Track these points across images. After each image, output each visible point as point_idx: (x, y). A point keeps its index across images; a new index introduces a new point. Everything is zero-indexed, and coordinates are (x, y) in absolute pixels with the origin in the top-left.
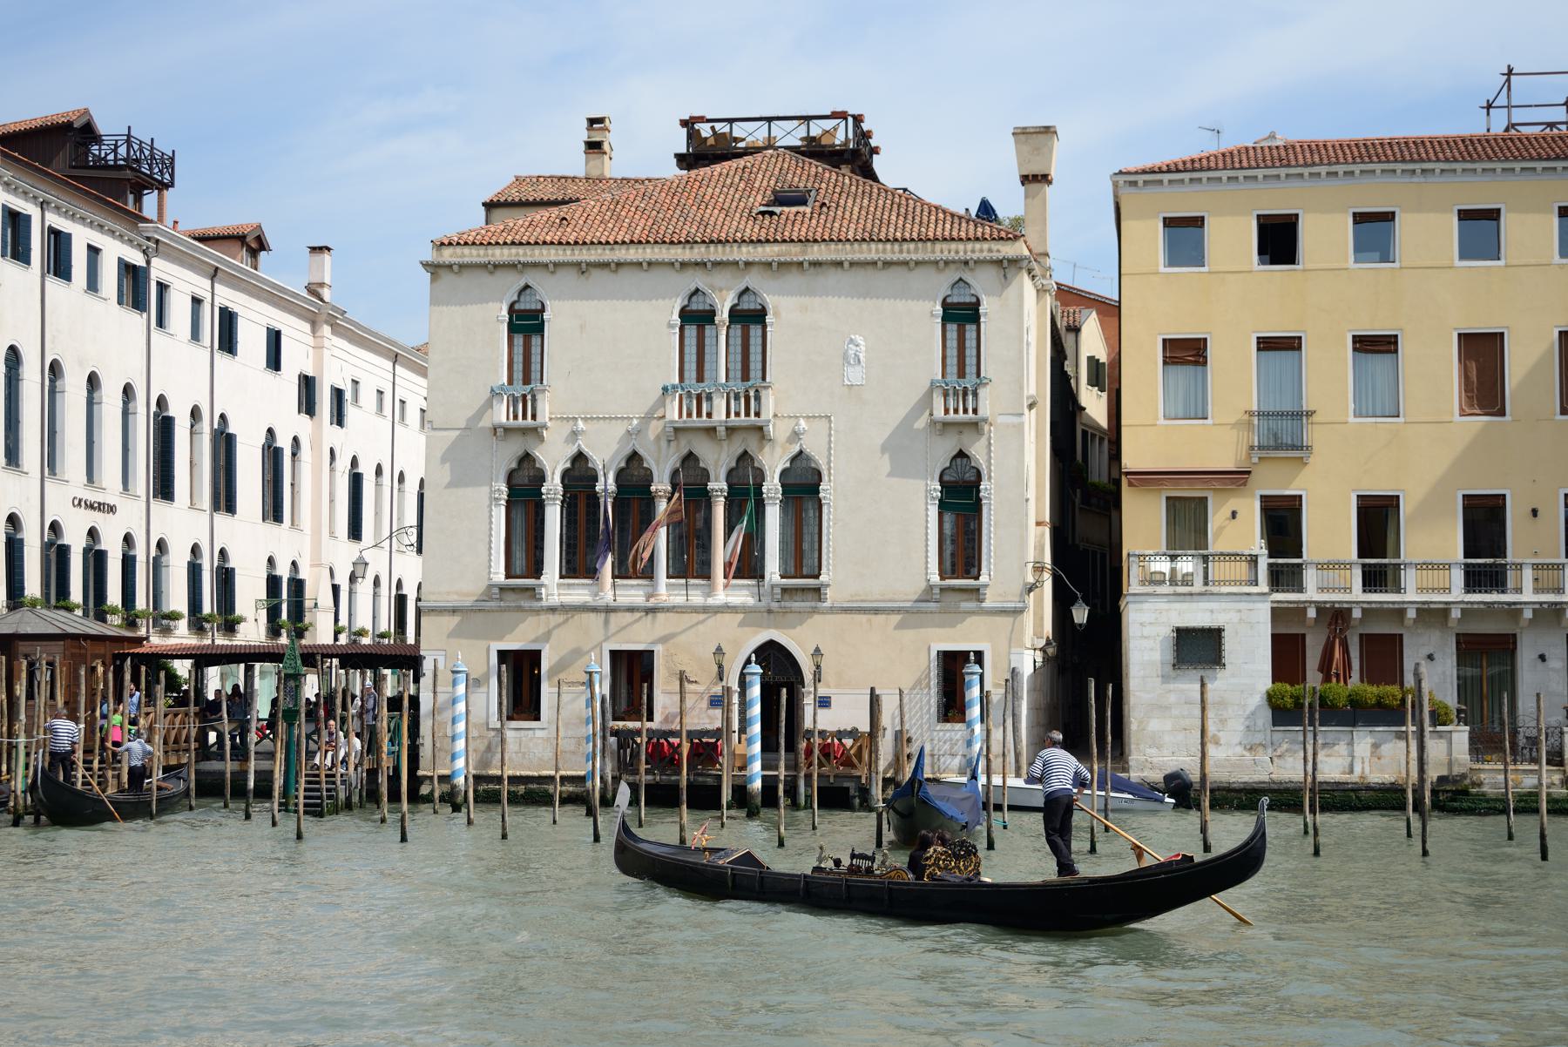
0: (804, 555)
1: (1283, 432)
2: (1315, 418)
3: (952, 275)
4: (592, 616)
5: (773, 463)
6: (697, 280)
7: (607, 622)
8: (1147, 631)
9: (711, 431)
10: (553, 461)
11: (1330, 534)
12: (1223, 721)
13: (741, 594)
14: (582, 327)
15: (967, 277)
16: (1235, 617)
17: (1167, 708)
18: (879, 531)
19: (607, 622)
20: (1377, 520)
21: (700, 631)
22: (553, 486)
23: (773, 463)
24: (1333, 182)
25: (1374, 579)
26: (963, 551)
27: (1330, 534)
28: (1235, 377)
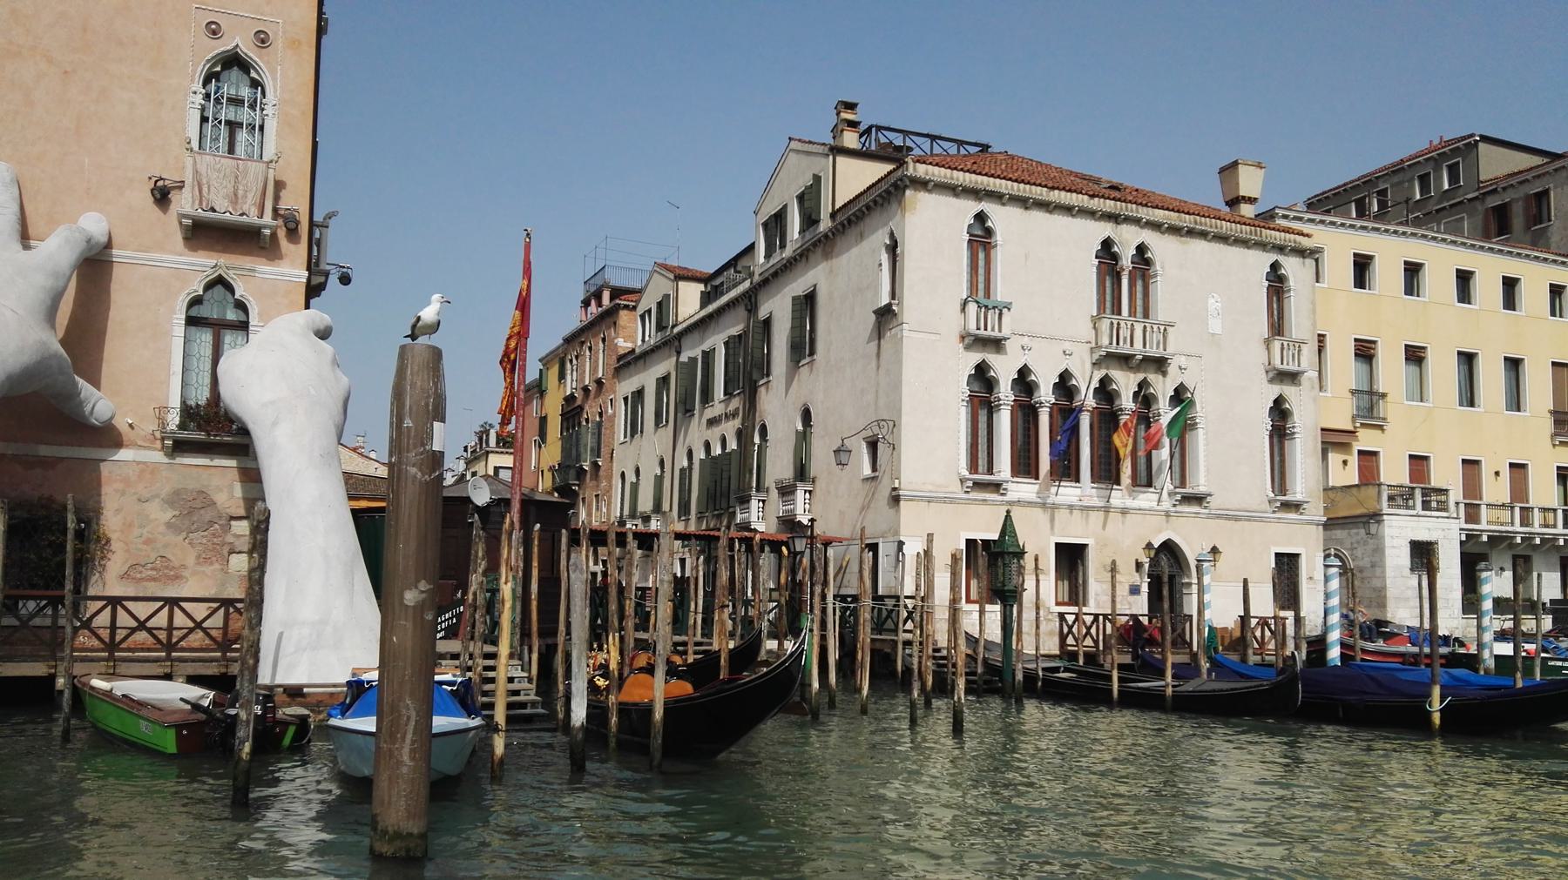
2: (1389, 398)
5: (1162, 388)
6: (1105, 230)
7: (1052, 520)
13: (1146, 499)
14: (1026, 257)
17: (1407, 599)
19: (1052, 520)
21: (1118, 527)
22: (1005, 392)
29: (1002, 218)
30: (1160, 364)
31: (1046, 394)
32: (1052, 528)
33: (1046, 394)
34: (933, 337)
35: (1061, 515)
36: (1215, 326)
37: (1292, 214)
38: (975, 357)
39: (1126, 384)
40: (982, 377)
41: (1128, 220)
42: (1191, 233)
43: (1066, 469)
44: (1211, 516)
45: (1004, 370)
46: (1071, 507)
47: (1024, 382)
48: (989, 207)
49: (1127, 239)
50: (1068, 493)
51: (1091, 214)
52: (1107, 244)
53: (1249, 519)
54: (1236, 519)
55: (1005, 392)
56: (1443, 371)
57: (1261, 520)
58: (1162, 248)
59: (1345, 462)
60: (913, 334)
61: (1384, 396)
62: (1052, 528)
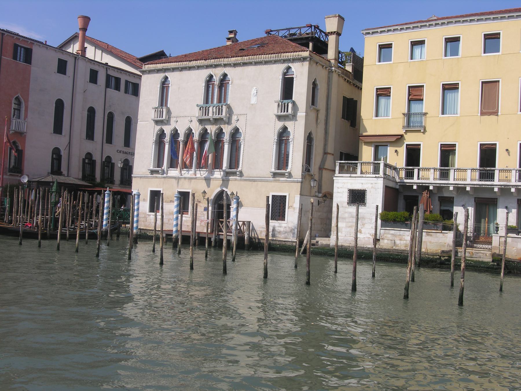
0: (234, 162)
1: (412, 121)
3: (285, 65)
4: (174, 180)
5: (227, 130)
8: (339, 190)
9: (209, 120)
10: (168, 130)
11: (430, 158)
12: (363, 225)
15: (290, 65)
16: (370, 186)
18: (257, 153)
20: (447, 153)
22: (167, 139)
23: (227, 130)
24: (438, 27)
25: (444, 175)
26: (282, 160)
27: (430, 158)
28: (398, 101)
29: (171, 76)
30: (229, 122)
31: (181, 138)
32: (178, 186)
33: (181, 138)
34: (147, 122)
35: (181, 181)
36: (253, 100)
37: (371, 31)
38: (158, 128)
39: (212, 129)
40: (161, 135)
41: (216, 66)
42: (245, 64)
43: (173, 164)
44: (241, 180)
45: (168, 130)
46: (185, 178)
47: (175, 134)
48: (167, 74)
49: (217, 73)
50: (186, 173)
51: (199, 67)
52: (211, 77)
53: (261, 181)
54: (254, 181)
55: (167, 139)
56: (469, 97)
57: (267, 181)
58: (231, 72)
59: (396, 151)
60: (141, 123)
61: (425, 114)
62: (178, 186)
